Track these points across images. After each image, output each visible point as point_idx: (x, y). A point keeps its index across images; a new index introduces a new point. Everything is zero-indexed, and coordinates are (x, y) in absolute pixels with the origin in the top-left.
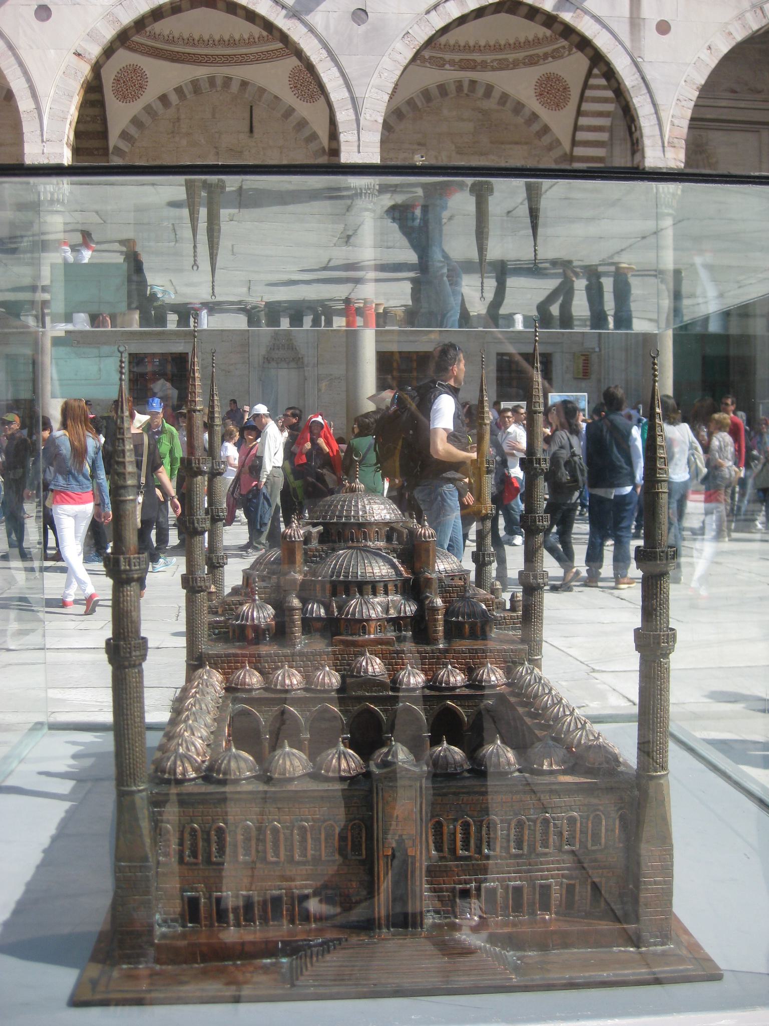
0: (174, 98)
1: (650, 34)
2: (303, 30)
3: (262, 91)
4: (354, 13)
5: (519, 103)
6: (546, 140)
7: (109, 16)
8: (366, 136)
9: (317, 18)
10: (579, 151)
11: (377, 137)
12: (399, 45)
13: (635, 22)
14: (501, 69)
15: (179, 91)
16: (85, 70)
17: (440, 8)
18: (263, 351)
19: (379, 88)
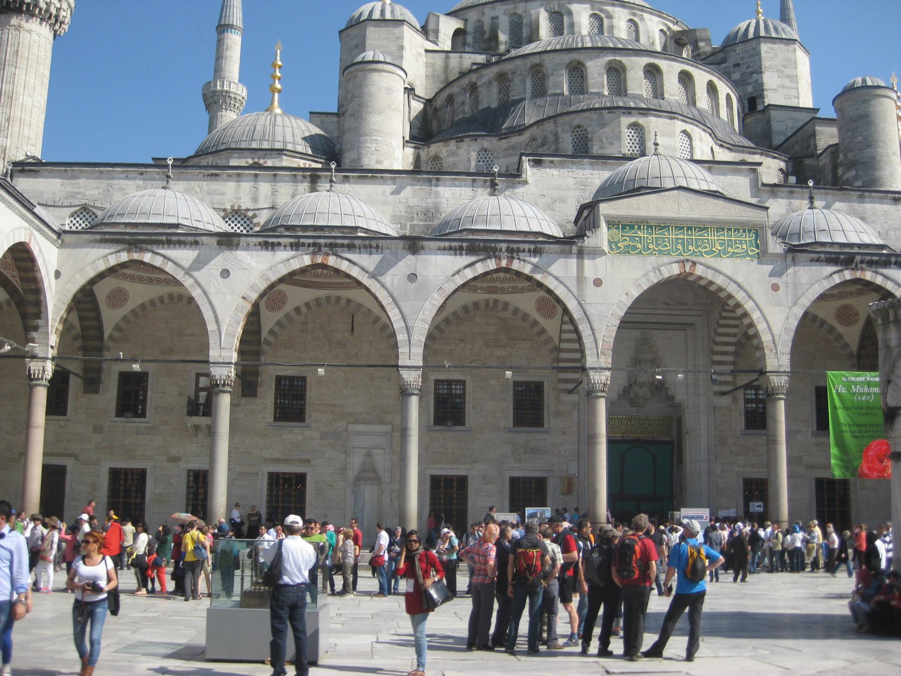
0: (304, 309)
1: (590, 288)
2: (379, 286)
3: (360, 306)
4: (409, 276)
5: (525, 314)
6: (543, 337)
7: (264, 276)
8: (414, 350)
9: (387, 279)
10: (564, 346)
11: (421, 350)
12: (435, 295)
13: (580, 279)
14: (514, 293)
15: (307, 305)
16: (248, 307)
17: (461, 273)
18: (355, 473)
19: (423, 321)
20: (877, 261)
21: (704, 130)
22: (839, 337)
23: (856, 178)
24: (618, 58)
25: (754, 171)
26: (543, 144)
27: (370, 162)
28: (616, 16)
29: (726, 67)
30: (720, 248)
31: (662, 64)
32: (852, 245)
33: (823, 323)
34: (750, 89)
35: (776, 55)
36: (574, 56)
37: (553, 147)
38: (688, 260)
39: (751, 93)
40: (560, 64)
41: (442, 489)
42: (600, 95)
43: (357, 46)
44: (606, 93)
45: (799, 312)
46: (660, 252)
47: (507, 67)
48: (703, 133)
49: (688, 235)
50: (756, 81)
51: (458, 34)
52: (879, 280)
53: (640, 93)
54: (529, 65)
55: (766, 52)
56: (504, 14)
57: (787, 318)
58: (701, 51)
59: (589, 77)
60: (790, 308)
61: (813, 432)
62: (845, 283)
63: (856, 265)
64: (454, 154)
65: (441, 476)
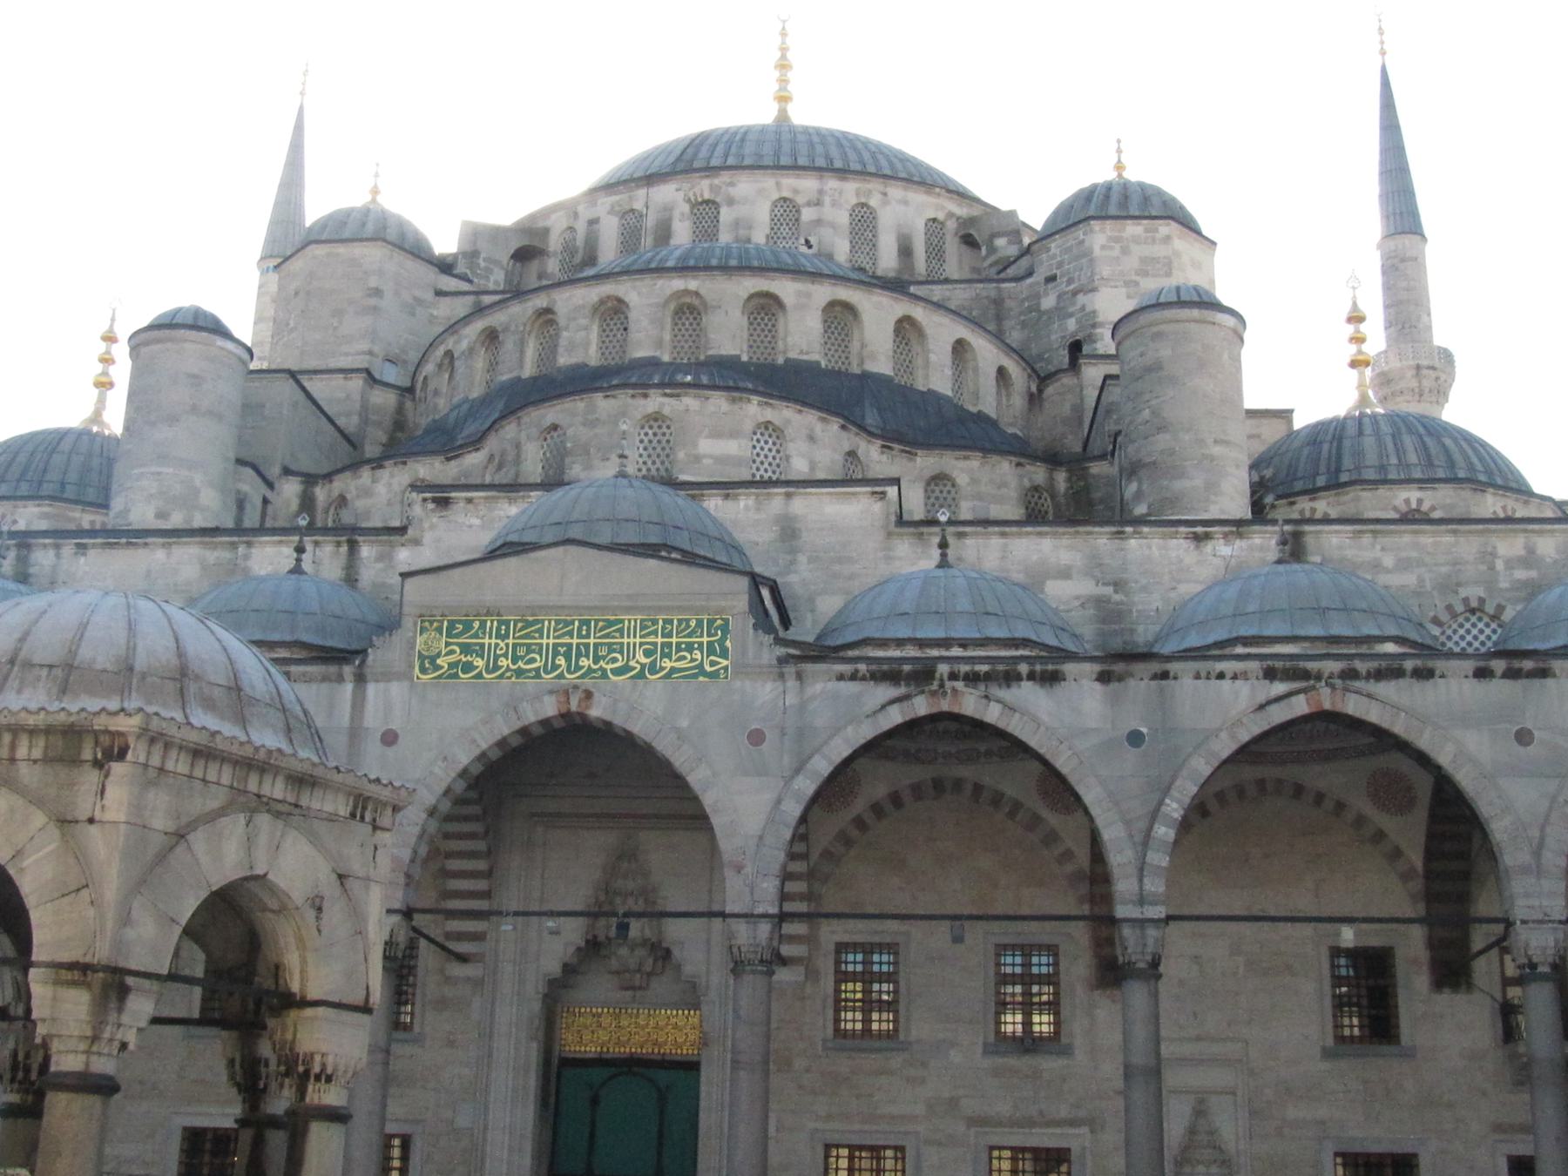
1: (373, 747)
20: (986, 673)
21: (823, 420)
22: (1051, 838)
23: (1139, 495)
24: (693, 284)
25: (884, 493)
26: (500, 467)
27: (142, 514)
28: (827, 200)
29: (1031, 286)
30: (644, 660)
31: (786, 288)
32: (946, 643)
33: (1017, 806)
34: (1071, 324)
35: (1125, 251)
36: (608, 289)
37: (513, 472)
38: (576, 687)
39: (1073, 335)
40: (583, 307)
41: (207, 1158)
42: (653, 363)
43: (296, 294)
44: (666, 358)
45: (807, 786)
46: (520, 673)
47: (497, 319)
48: (818, 427)
49: (580, 636)
50: (1083, 308)
51: (524, 255)
52: (992, 714)
53: (733, 352)
54: (530, 312)
55: (1103, 247)
56: (611, 212)
57: (779, 801)
58: (1001, 254)
59: (632, 327)
60: (788, 781)
61: (985, 1045)
62: (911, 727)
63: (942, 686)
64: (367, 493)
65: (205, 1130)
